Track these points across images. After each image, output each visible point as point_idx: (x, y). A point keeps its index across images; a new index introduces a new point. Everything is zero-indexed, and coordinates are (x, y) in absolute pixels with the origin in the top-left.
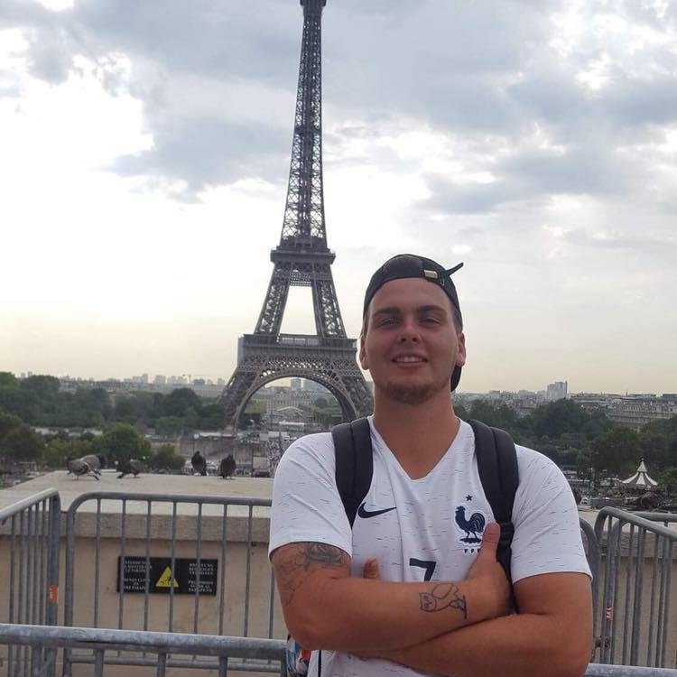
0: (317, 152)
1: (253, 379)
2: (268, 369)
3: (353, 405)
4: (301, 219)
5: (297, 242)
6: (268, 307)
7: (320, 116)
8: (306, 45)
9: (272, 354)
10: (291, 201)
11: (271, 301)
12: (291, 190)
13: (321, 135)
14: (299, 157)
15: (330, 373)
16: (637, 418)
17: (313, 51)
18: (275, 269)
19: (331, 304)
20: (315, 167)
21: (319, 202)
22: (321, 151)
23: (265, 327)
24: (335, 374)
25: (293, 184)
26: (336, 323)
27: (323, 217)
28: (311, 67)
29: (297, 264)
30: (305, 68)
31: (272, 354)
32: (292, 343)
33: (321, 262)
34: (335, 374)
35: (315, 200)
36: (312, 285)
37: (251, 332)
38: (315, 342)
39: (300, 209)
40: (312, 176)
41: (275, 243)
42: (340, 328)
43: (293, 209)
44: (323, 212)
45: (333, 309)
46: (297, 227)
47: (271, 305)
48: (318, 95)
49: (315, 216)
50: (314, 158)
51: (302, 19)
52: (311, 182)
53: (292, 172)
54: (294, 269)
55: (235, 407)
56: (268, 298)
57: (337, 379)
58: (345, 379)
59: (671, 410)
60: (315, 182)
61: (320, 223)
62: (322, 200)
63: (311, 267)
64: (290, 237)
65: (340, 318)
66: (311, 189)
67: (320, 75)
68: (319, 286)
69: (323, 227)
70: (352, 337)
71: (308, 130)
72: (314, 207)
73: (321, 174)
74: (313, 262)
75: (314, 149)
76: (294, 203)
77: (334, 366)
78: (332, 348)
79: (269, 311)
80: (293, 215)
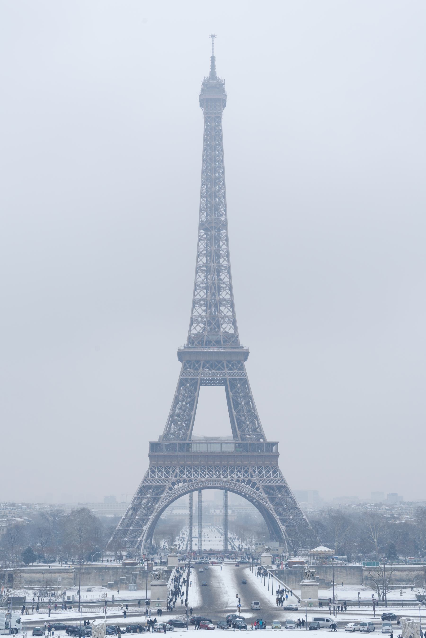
0: (224, 247)
1: (162, 493)
2: (179, 482)
3: (277, 517)
6: (177, 411)
7: (225, 211)
8: (207, 145)
9: (182, 463)
10: (198, 296)
11: (180, 404)
12: (198, 285)
13: (227, 229)
14: (205, 252)
18: (185, 367)
19: (247, 403)
21: (228, 296)
23: (173, 434)
24: (255, 484)
26: (254, 424)
27: (233, 312)
28: (213, 165)
29: (207, 362)
30: (207, 167)
32: (204, 449)
34: (255, 484)
35: (225, 294)
36: (225, 384)
40: (218, 271)
41: (182, 342)
42: (258, 430)
44: (232, 306)
47: (180, 408)
49: (225, 310)
50: (221, 252)
51: (203, 120)
52: (218, 276)
53: (198, 268)
55: (141, 526)
56: (177, 400)
58: (268, 489)
61: (231, 318)
62: (232, 295)
63: (223, 365)
67: (223, 172)
68: (233, 386)
69: (234, 323)
70: (269, 439)
71: (213, 225)
73: (229, 268)
75: (221, 244)
76: (202, 299)
77: (253, 474)
78: (249, 454)
79: (178, 415)
80: (200, 311)
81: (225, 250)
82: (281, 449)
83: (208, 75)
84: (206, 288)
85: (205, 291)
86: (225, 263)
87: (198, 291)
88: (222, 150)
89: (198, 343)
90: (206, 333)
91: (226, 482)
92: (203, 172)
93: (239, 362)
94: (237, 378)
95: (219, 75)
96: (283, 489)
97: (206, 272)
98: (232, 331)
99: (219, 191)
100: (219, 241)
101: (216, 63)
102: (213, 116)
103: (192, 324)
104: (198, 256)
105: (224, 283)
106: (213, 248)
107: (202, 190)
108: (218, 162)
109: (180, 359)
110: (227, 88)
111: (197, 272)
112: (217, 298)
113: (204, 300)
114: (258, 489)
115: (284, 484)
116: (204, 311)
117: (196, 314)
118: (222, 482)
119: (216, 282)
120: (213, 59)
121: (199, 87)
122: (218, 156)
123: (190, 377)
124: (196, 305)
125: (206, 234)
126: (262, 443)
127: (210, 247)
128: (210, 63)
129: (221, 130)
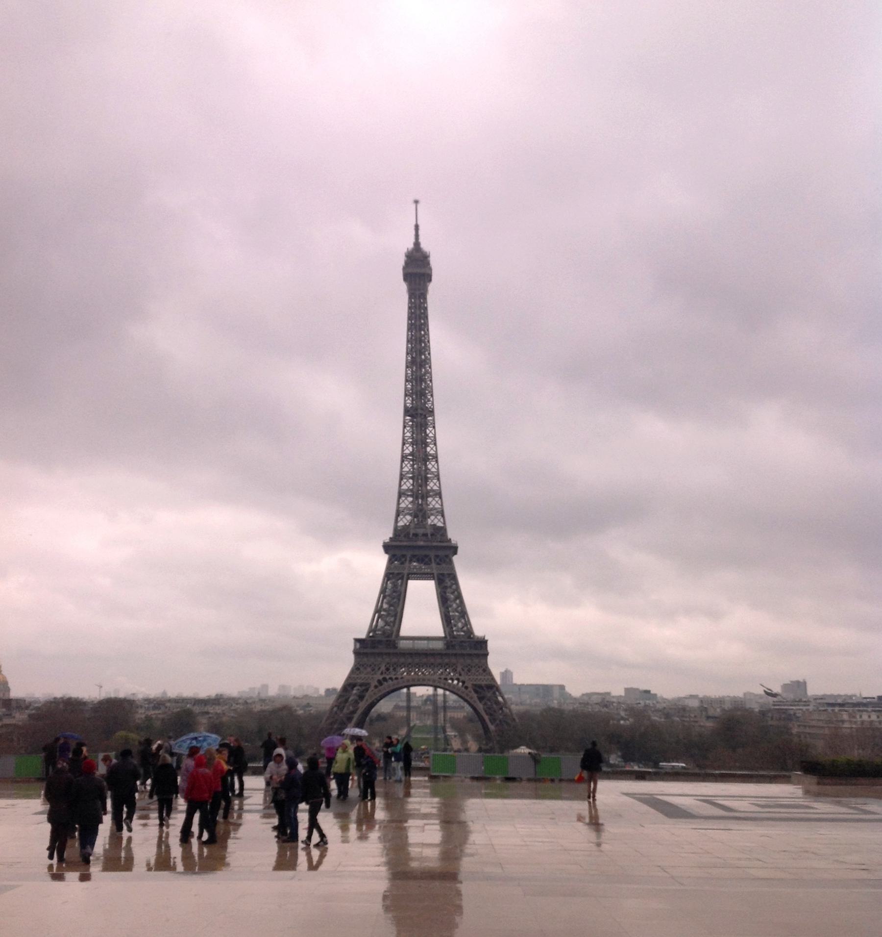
3: (486, 718)
5: (412, 532)
6: (385, 606)
7: (432, 396)
10: (404, 487)
13: (433, 415)
15: (458, 679)
16: (823, 727)
17: (420, 331)
18: (390, 562)
23: (379, 630)
28: (418, 347)
29: (414, 556)
31: (387, 660)
32: (411, 646)
33: (441, 553)
35: (432, 485)
37: (363, 636)
38: (440, 645)
41: (388, 534)
44: (441, 498)
49: (433, 502)
52: (426, 465)
53: (404, 458)
54: (411, 561)
57: (466, 688)
59: (861, 717)
63: (430, 560)
71: (420, 411)
74: (432, 554)
75: (428, 432)
76: (408, 490)
77: (463, 673)
79: (385, 610)
80: (407, 502)
82: (490, 646)
83: (411, 246)
85: (411, 481)
86: (432, 452)
89: (405, 536)
90: (412, 525)
91: (434, 681)
92: (407, 354)
93: (447, 556)
94: (445, 572)
95: (425, 246)
96: (492, 687)
97: (413, 460)
98: (440, 524)
99: (425, 375)
100: (426, 429)
101: (420, 232)
102: (417, 293)
103: (398, 515)
104: (404, 444)
106: (419, 437)
107: (406, 374)
109: (386, 552)
110: (434, 262)
111: (402, 461)
112: (424, 491)
113: (411, 490)
114: (466, 688)
115: (492, 683)
116: (411, 503)
117: (403, 505)
118: (429, 680)
119: (423, 473)
120: (417, 227)
121: (401, 261)
122: (424, 336)
123: (396, 572)
125: (411, 421)
128: (414, 232)
129: (426, 309)
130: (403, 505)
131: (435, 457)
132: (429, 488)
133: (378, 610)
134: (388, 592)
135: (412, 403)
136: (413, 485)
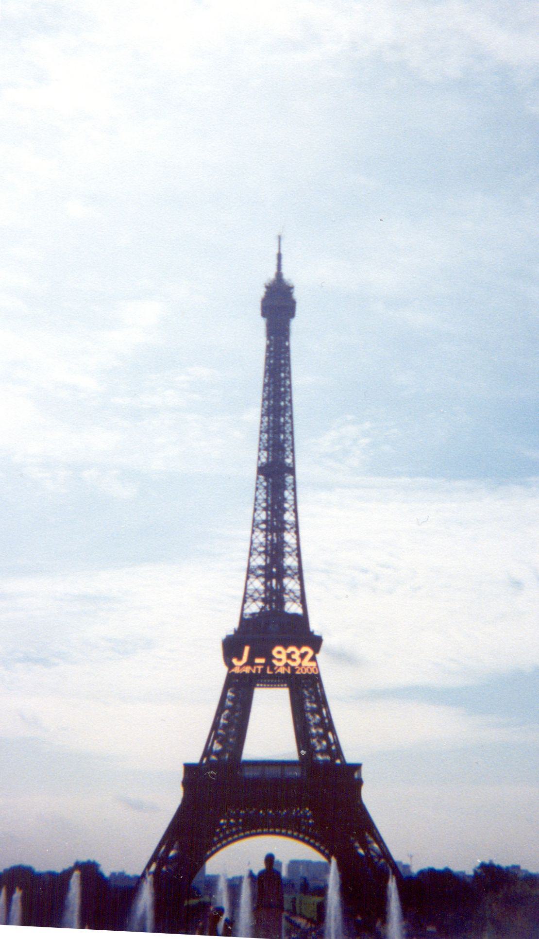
4: (268, 589)
7: (293, 451)
10: (254, 564)
11: (227, 712)
12: (255, 549)
14: (264, 505)
20: (288, 517)
22: (295, 496)
25: (256, 541)
26: (328, 740)
35: (290, 561)
37: (195, 756)
38: (296, 773)
39: (268, 576)
40: (284, 529)
41: (231, 625)
42: (333, 748)
43: (258, 577)
45: (322, 718)
46: (264, 600)
48: (288, 425)
49: (291, 584)
50: (286, 506)
52: (282, 538)
53: (255, 525)
60: (289, 537)
61: (298, 593)
64: (253, 614)
65: (334, 733)
66: (283, 547)
72: (289, 572)
76: (260, 567)
79: (225, 727)
80: (257, 584)
81: (292, 502)
82: (366, 774)
84: (265, 552)
85: (264, 556)
87: (254, 557)
88: (289, 373)
92: (264, 400)
95: (288, 276)
97: (266, 530)
98: (300, 611)
103: (244, 601)
104: (255, 510)
105: (289, 547)
108: (284, 386)
110: (297, 295)
111: (253, 532)
121: (261, 292)
122: (286, 378)
124: (251, 576)
125: (266, 480)
126: (337, 765)
127: (272, 499)
130: (250, 587)
131: (296, 525)
132: (285, 565)
133: (215, 726)
134: (229, 703)
135: (268, 459)
136: (266, 560)
